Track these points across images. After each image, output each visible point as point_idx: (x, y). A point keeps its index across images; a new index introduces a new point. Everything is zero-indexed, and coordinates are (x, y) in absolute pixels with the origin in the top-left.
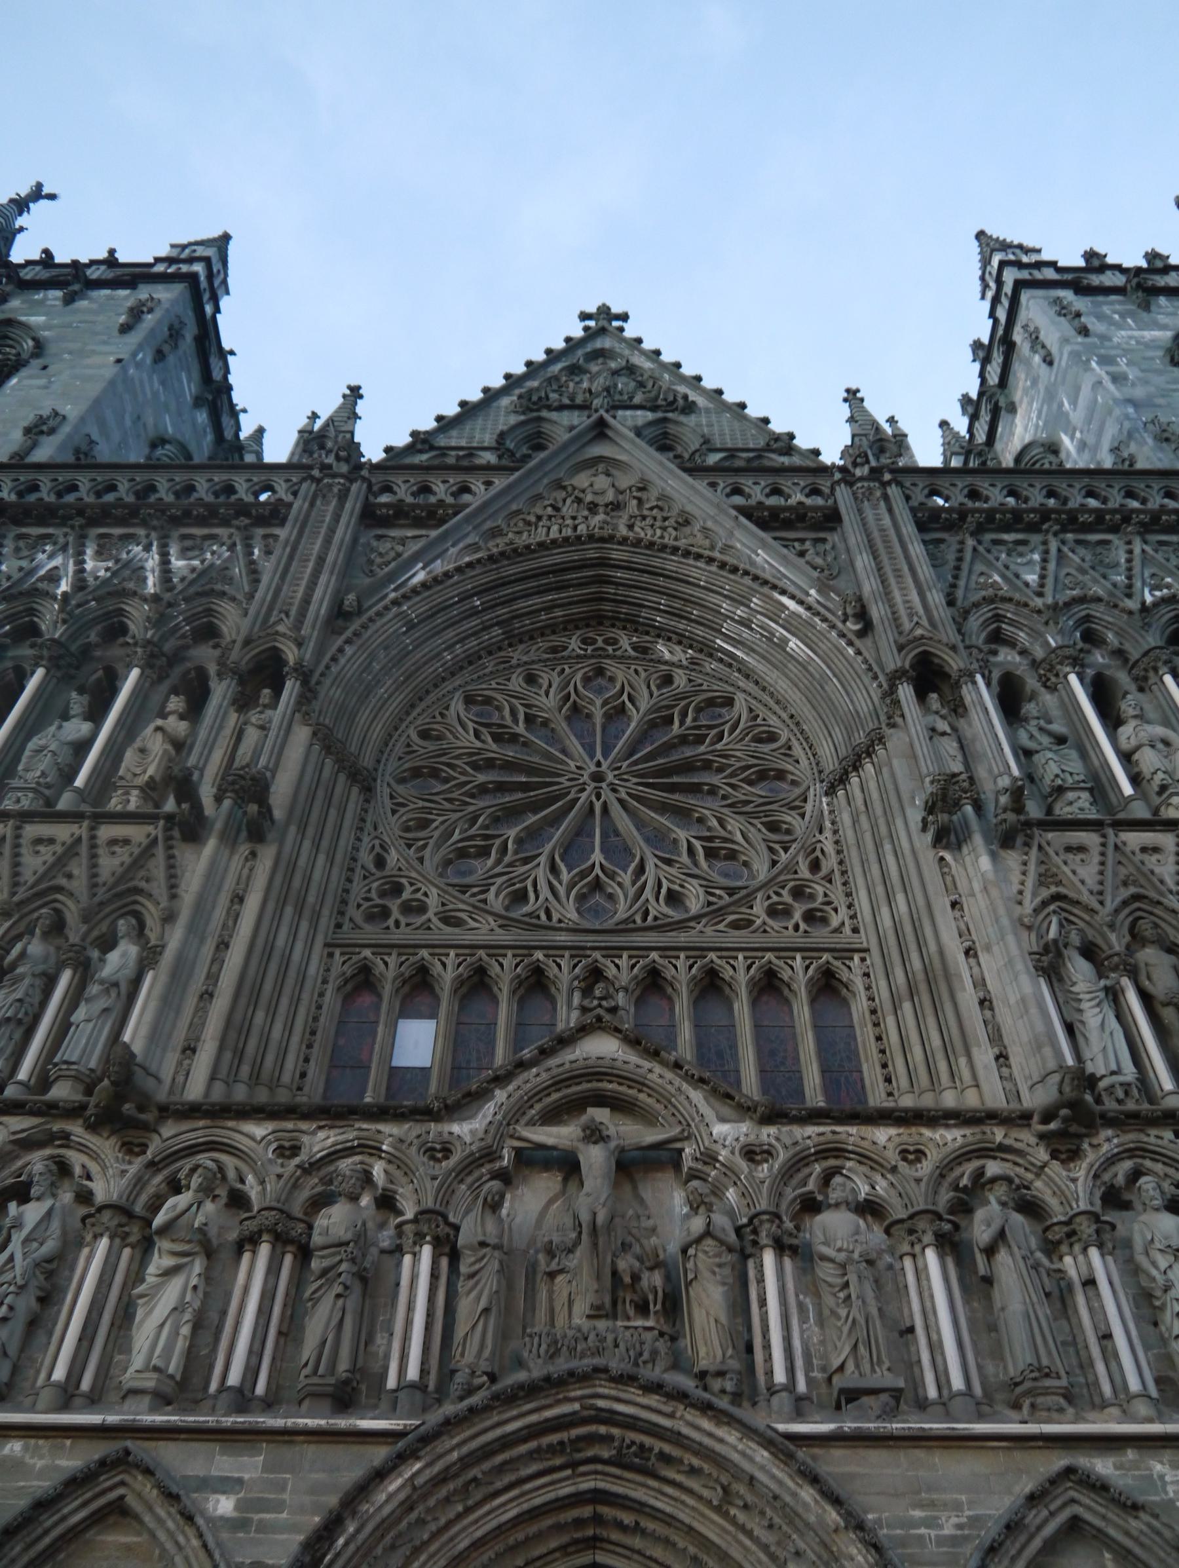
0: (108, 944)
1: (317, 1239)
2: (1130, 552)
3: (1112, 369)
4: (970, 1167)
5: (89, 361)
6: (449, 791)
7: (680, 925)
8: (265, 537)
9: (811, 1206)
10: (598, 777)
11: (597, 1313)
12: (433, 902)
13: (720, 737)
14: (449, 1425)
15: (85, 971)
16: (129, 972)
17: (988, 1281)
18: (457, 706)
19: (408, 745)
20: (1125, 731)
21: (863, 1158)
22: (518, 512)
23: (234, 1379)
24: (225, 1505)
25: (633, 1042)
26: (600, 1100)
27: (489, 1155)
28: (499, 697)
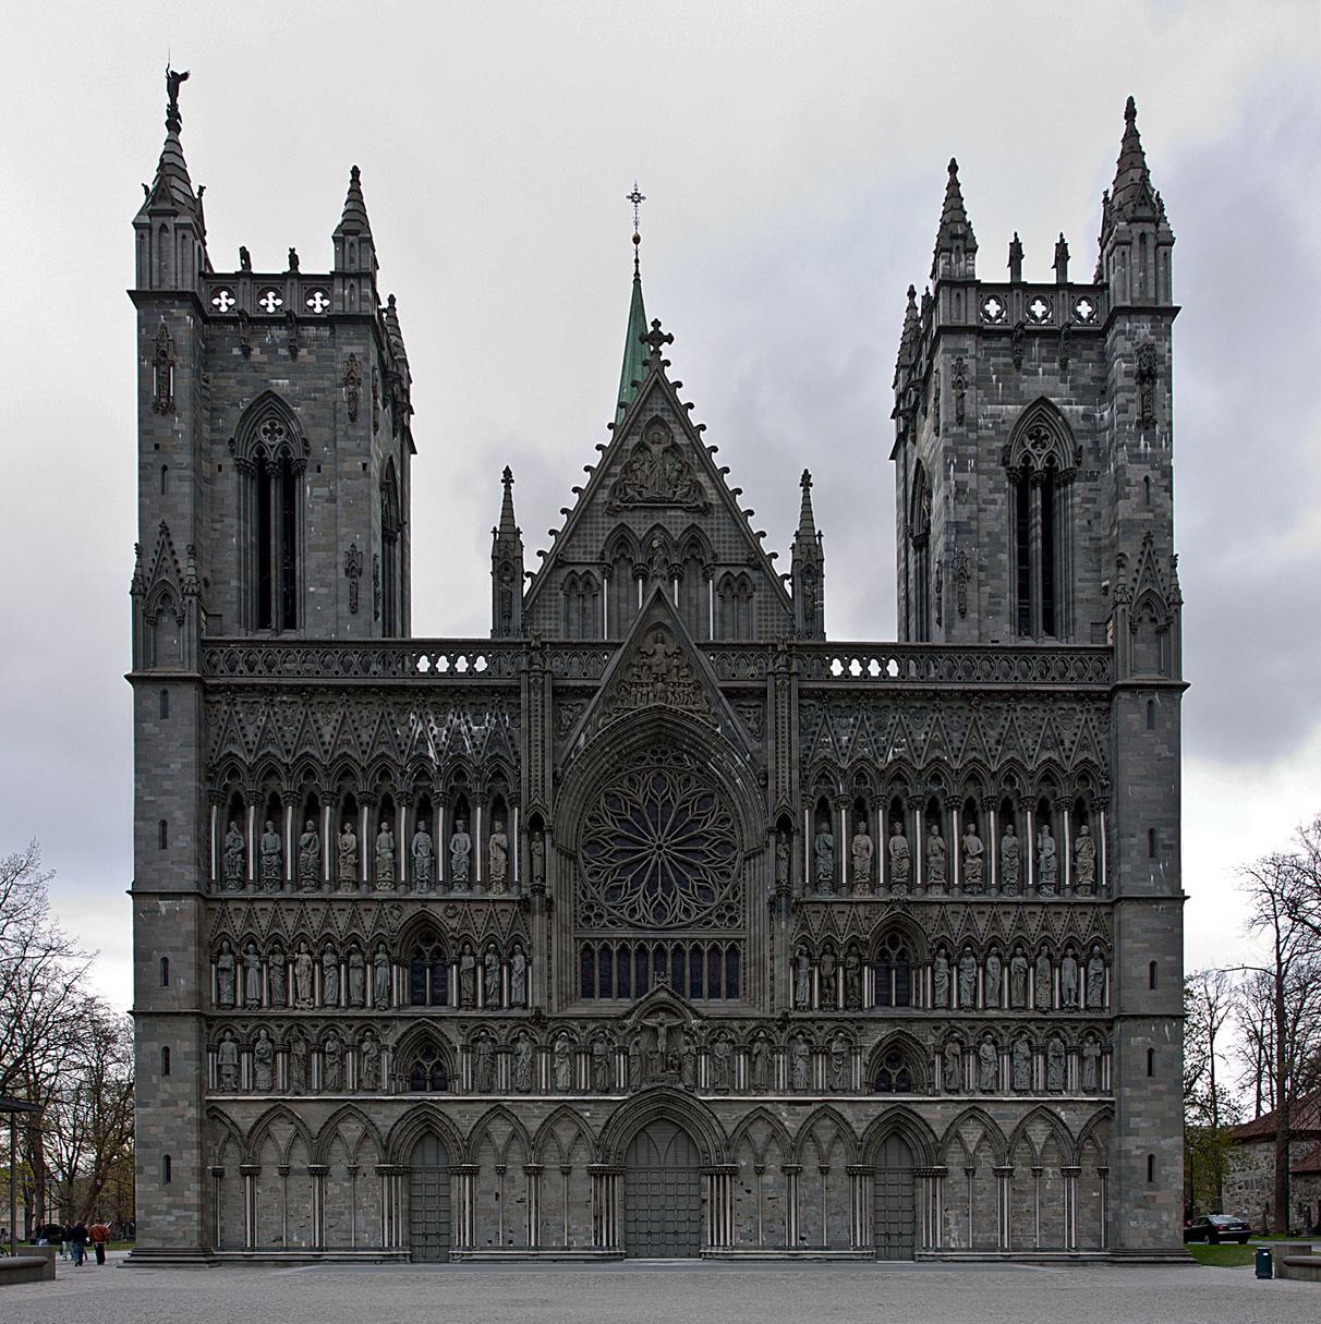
0: (512, 955)
1: (595, 1053)
2: (894, 718)
3: (961, 477)
4: (757, 1031)
5: (346, 467)
6: (604, 855)
7: (688, 926)
8: (509, 704)
9: (715, 1041)
10: (660, 847)
11: (662, 1071)
12: (605, 914)
13: (707, 819)
14: (632, 1098)
15: (511, 967)
16: (524, 967)
17: (755, 1062)
18: (603, 800)
19: (586, 827)
20: (857, 838)
21: (730, 1029)
22: (622, 681)
23: (583, 1087)
24: (588, 1114)
25: (672, 995)
26: (663, 1010)
27: (635, 1028)
28: (618, 793)
